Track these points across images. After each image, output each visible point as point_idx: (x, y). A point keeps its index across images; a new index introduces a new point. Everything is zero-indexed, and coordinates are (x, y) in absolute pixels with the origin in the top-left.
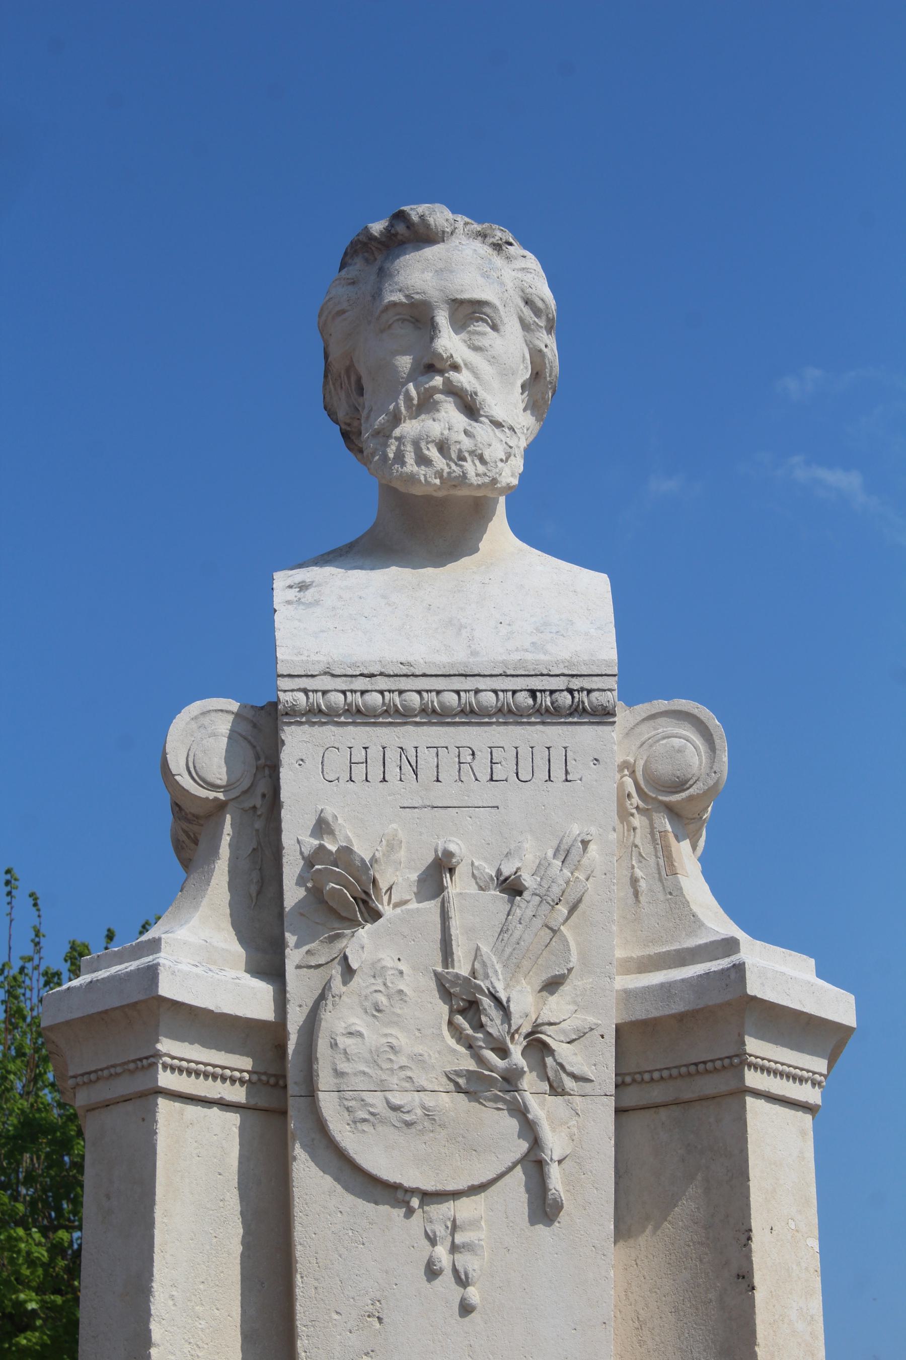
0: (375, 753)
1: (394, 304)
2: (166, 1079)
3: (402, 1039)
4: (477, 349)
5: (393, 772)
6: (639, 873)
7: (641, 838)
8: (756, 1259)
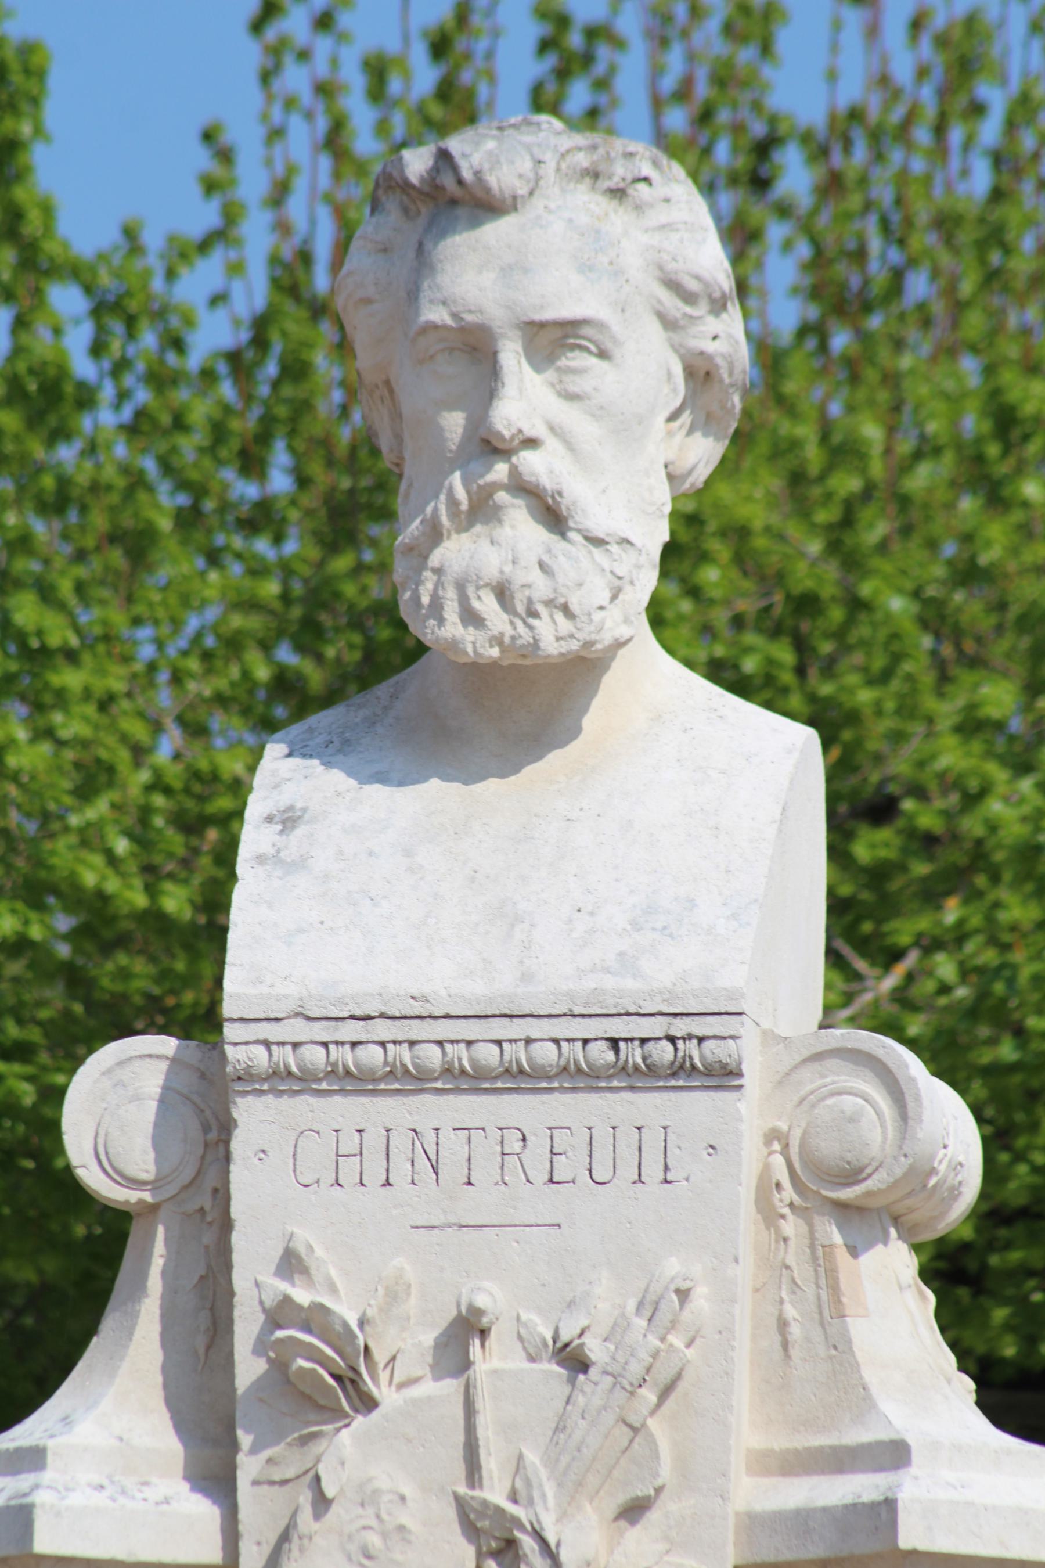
0: (374, 1139)
1: (433, 327)
5: (401, 1170)
7: (795, 1255)
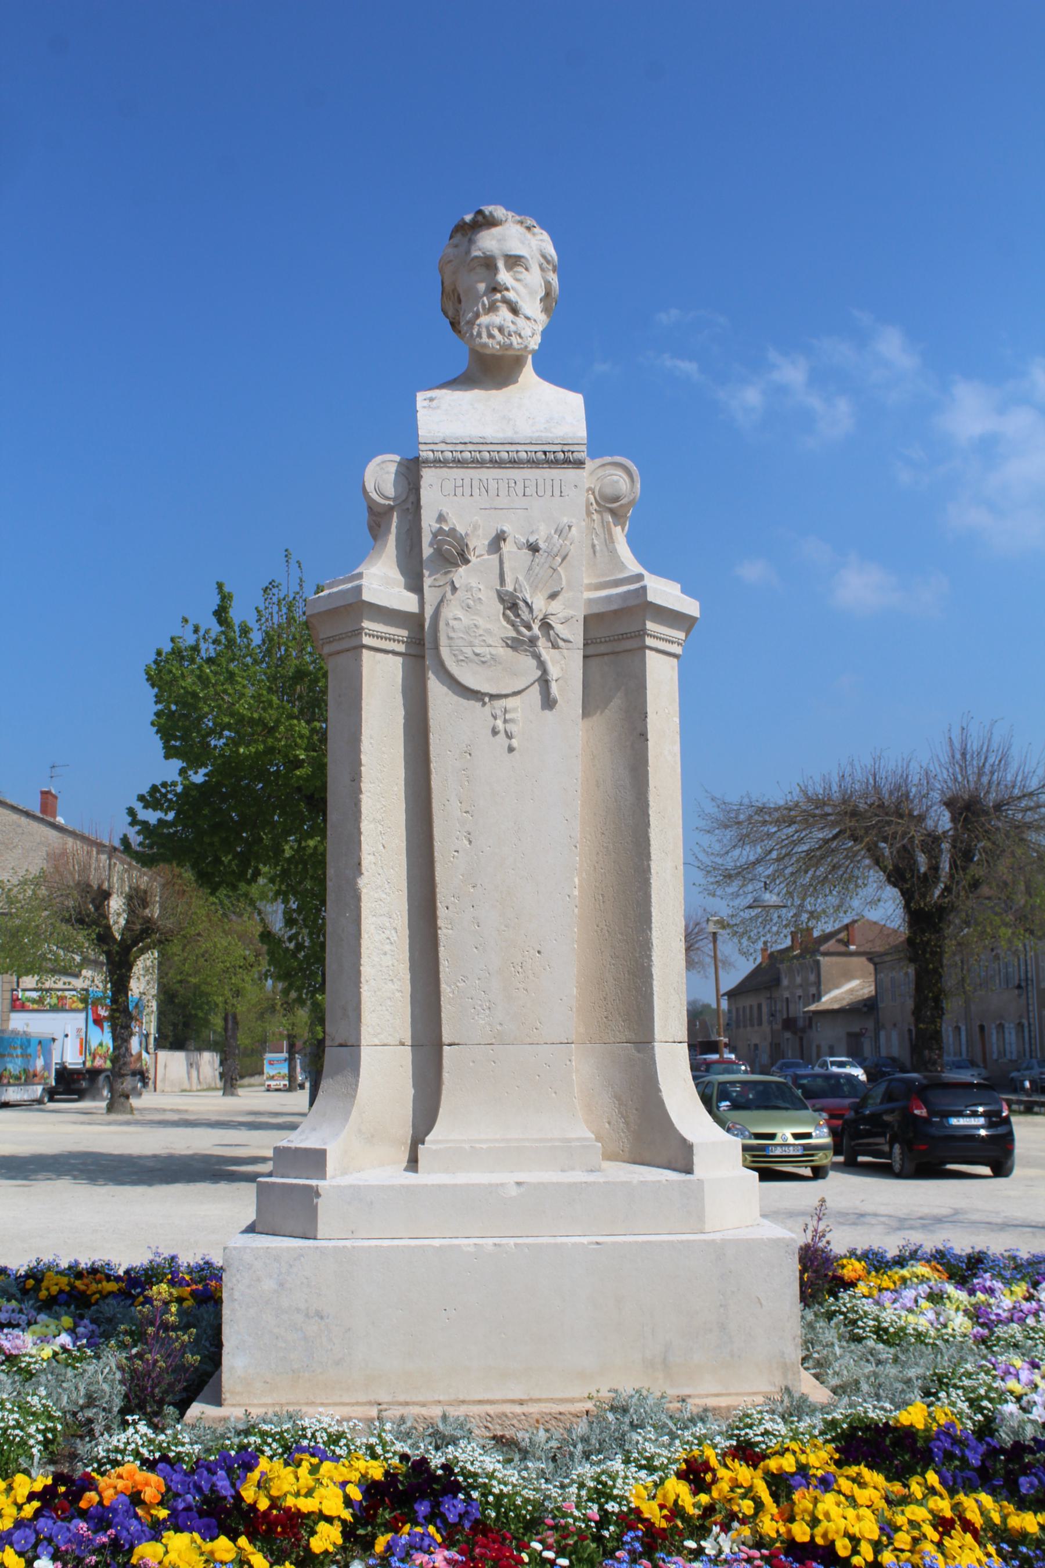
0: (467, 482)
1: (476, 257)
2: (366, 640)
3: (480, 621)
4: (518, 280)
5: (476, 491)
6: (596, 542)
7: (597, 525)
8: (649, 727)
